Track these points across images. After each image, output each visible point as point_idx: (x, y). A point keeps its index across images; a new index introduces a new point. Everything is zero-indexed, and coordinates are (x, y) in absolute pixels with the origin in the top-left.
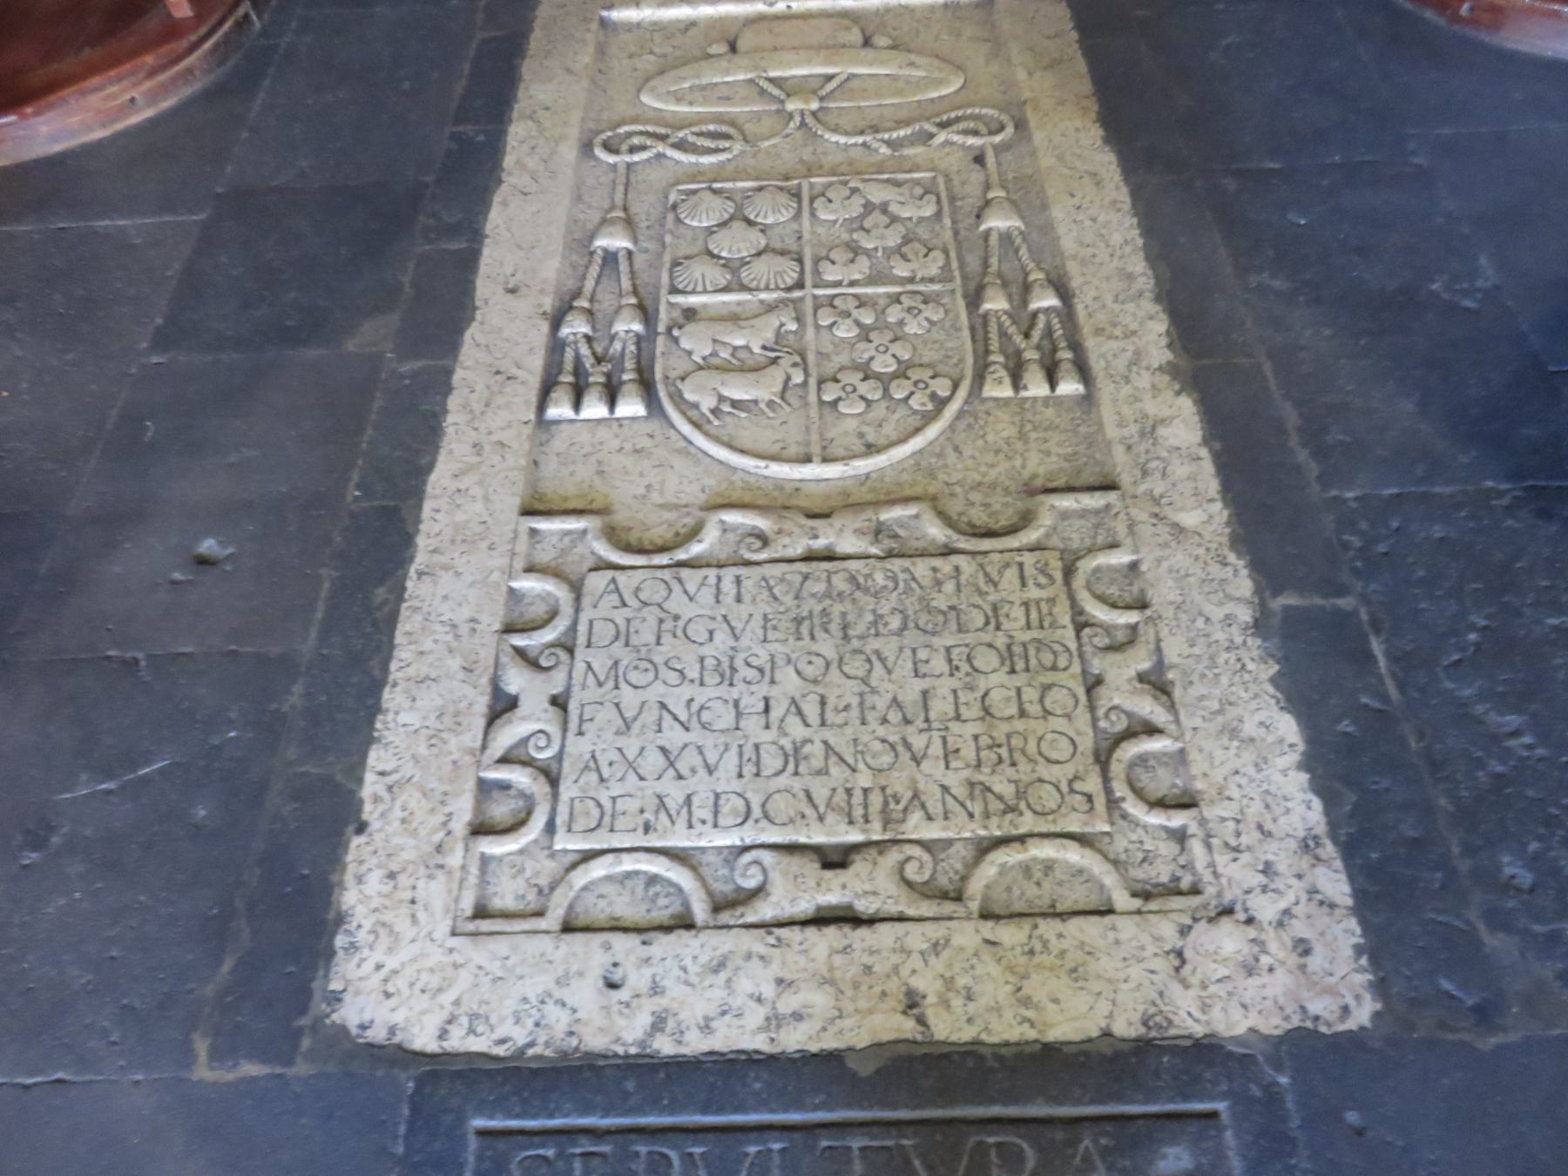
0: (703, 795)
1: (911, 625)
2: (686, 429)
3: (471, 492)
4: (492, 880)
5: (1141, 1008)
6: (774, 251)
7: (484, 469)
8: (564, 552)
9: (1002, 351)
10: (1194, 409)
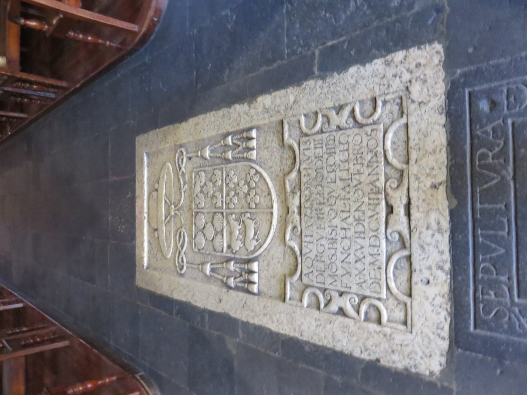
1: (320, 183)
2: (262, 250)
3: (278, 317)
6: (212, 220)
9: (243, 154)
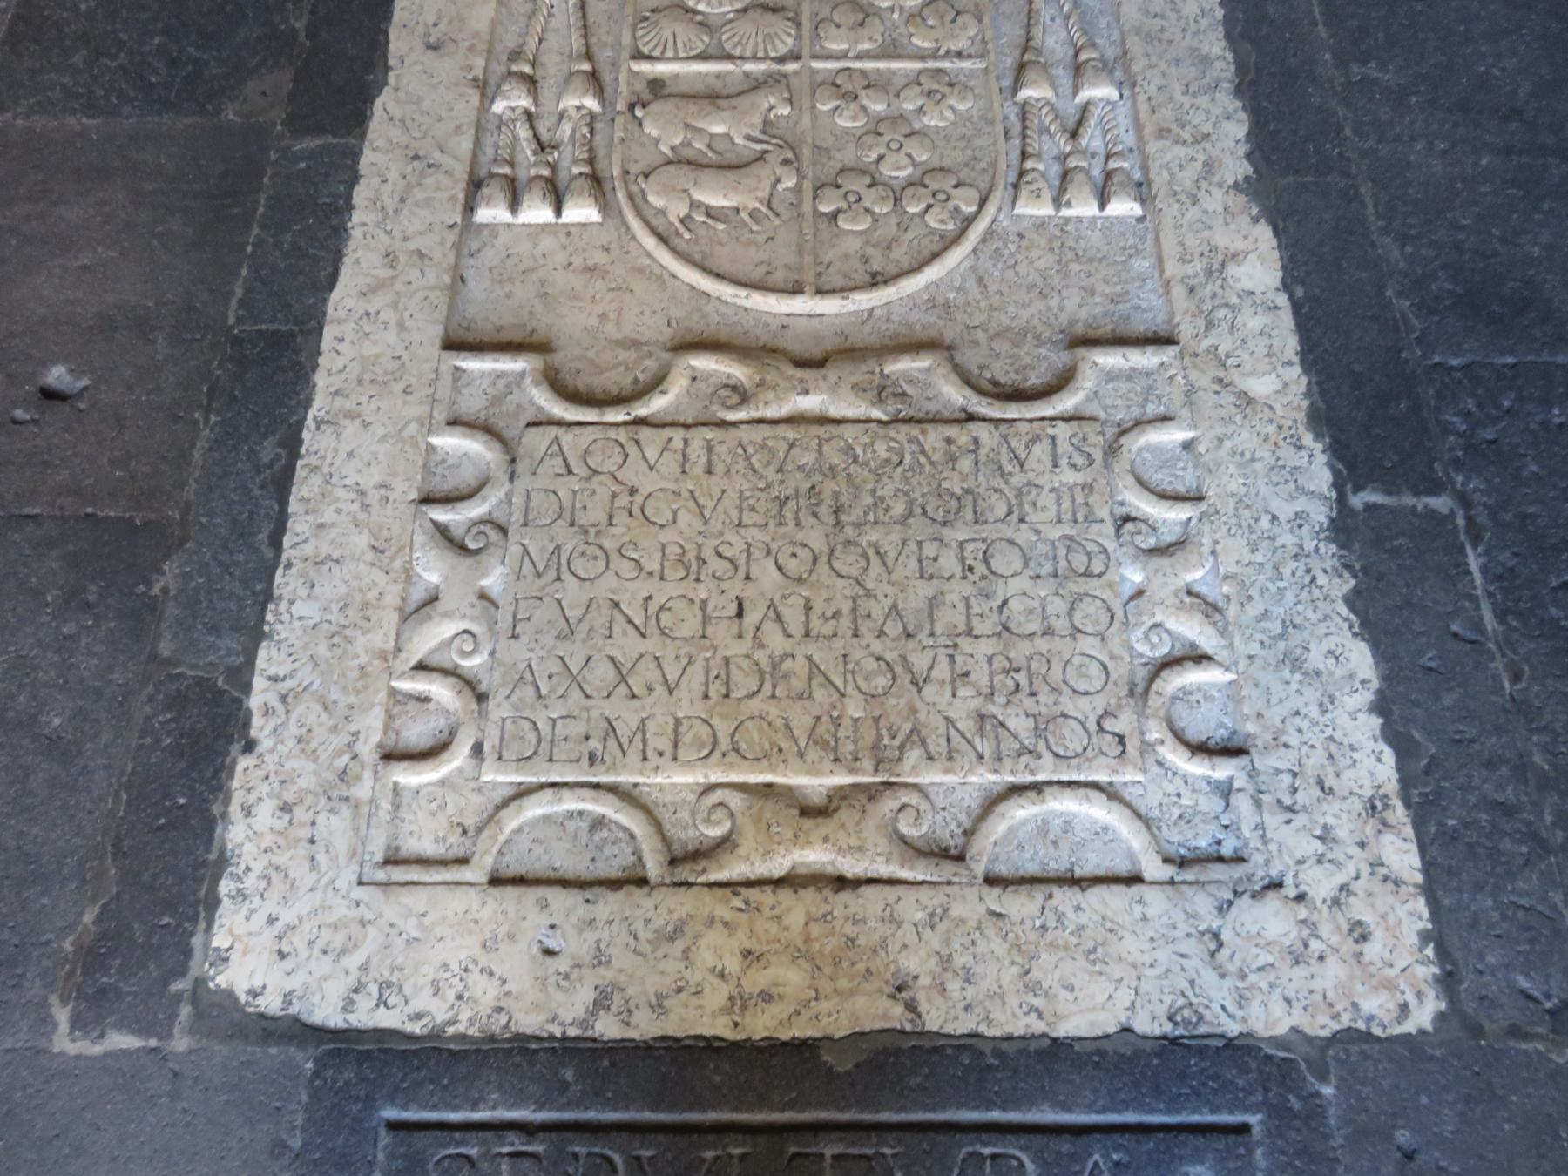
0: (661, 719)
2: (650, 242)
3: (382, 316)
4: (408, 817)
5: (1168, 999)
7: (399, 286)
8: (496, 401)
10: (1275, 243)
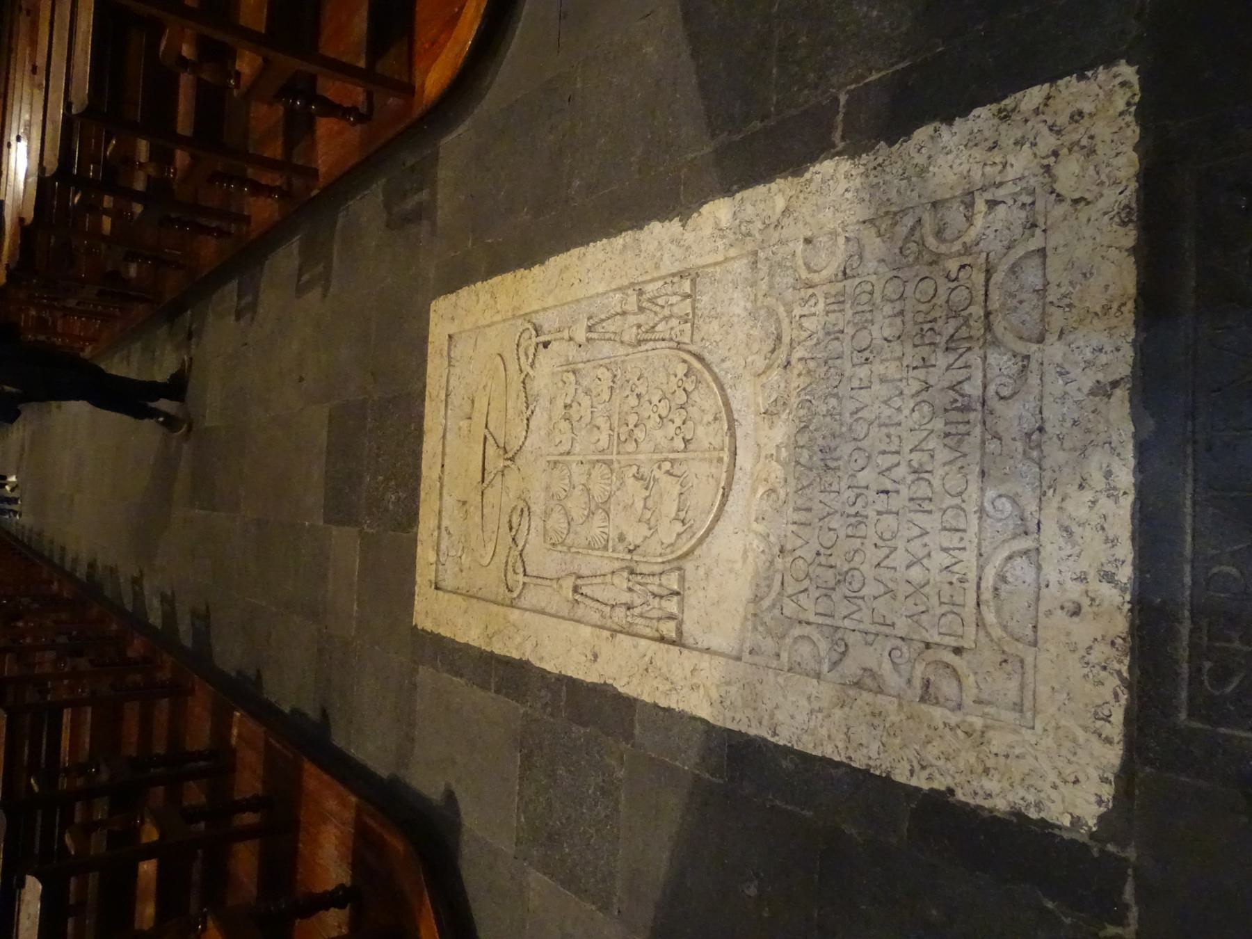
7: (708, 684)
